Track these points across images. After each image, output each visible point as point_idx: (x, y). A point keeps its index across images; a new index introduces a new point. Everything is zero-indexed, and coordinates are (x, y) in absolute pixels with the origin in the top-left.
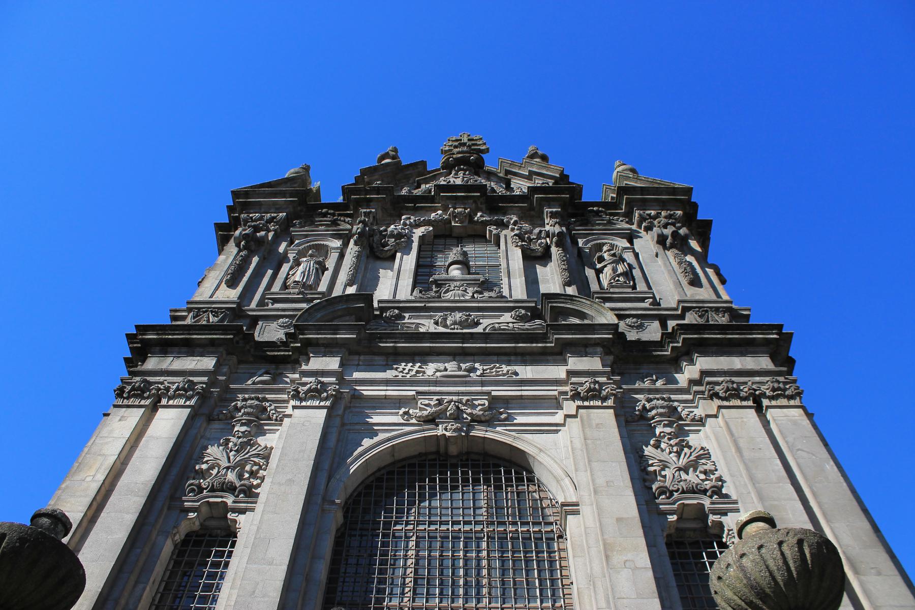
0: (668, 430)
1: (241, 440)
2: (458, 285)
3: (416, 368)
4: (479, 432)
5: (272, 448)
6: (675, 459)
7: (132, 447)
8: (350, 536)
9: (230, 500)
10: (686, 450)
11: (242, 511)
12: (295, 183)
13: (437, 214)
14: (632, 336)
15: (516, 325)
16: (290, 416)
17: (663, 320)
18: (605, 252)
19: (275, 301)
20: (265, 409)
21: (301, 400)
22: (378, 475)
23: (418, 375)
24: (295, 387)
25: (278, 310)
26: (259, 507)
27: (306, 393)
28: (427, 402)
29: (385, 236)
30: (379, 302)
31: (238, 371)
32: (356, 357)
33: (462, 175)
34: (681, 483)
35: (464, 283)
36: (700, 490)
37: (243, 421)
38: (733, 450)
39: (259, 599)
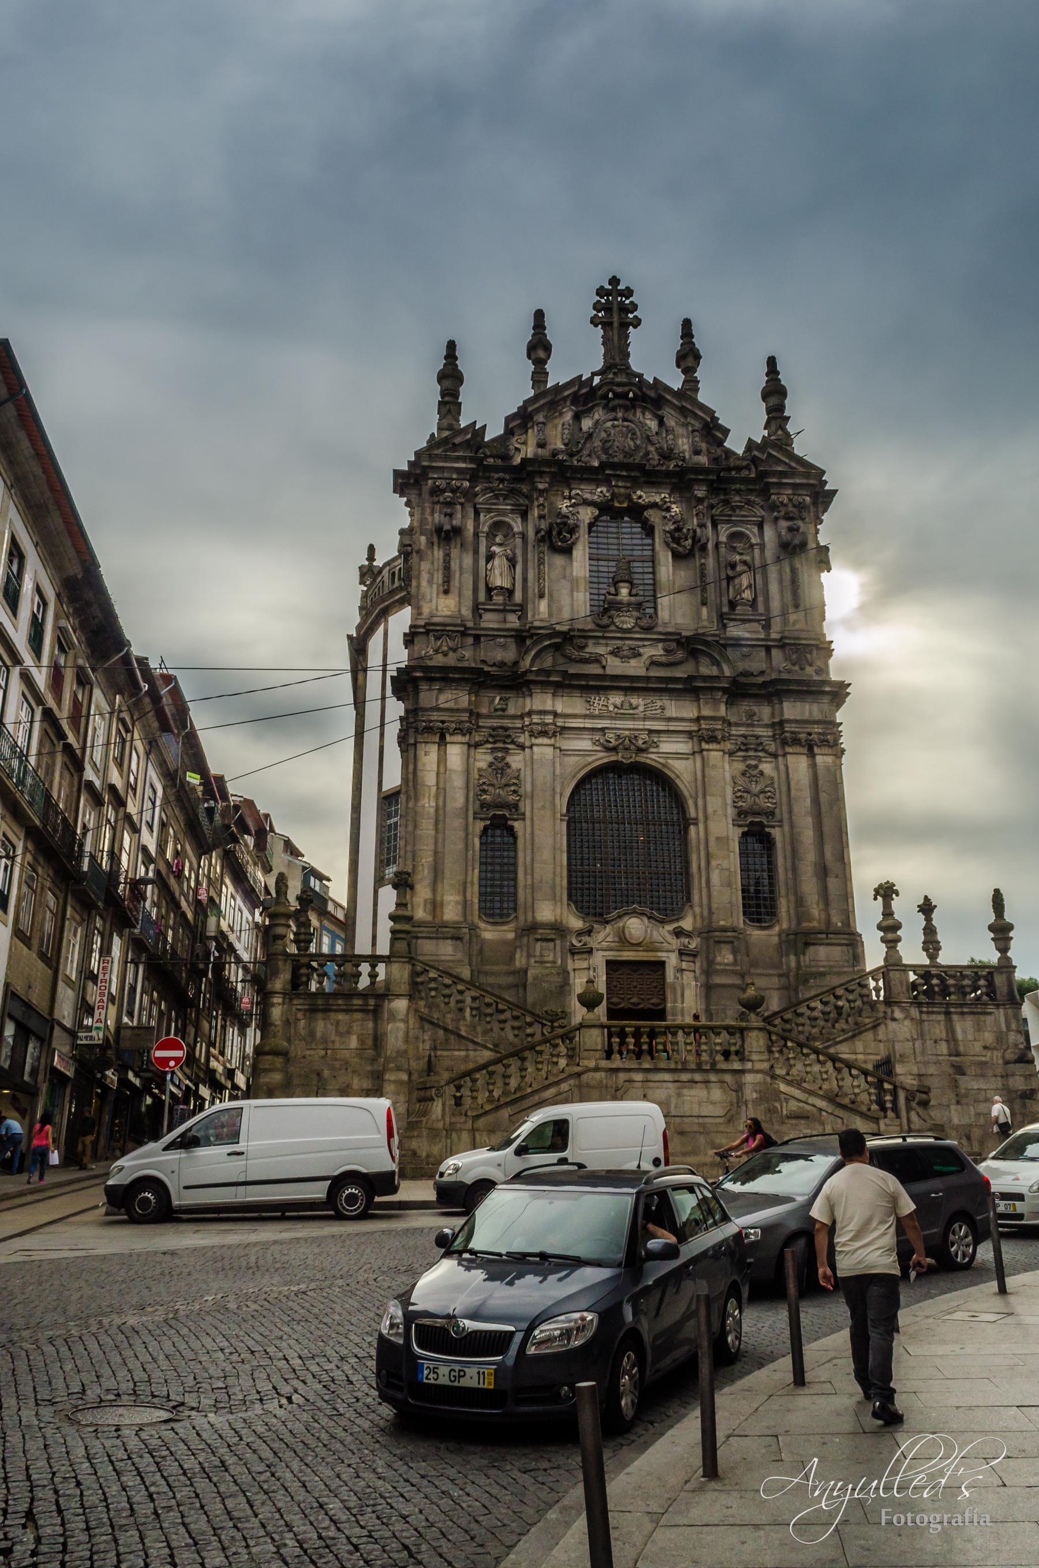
3: (601, 703)
4: (642, 758)
12: (466, 434)
17: (768, 649)
20: (509, 736)
26: (528, 822)
28: (611, 735)
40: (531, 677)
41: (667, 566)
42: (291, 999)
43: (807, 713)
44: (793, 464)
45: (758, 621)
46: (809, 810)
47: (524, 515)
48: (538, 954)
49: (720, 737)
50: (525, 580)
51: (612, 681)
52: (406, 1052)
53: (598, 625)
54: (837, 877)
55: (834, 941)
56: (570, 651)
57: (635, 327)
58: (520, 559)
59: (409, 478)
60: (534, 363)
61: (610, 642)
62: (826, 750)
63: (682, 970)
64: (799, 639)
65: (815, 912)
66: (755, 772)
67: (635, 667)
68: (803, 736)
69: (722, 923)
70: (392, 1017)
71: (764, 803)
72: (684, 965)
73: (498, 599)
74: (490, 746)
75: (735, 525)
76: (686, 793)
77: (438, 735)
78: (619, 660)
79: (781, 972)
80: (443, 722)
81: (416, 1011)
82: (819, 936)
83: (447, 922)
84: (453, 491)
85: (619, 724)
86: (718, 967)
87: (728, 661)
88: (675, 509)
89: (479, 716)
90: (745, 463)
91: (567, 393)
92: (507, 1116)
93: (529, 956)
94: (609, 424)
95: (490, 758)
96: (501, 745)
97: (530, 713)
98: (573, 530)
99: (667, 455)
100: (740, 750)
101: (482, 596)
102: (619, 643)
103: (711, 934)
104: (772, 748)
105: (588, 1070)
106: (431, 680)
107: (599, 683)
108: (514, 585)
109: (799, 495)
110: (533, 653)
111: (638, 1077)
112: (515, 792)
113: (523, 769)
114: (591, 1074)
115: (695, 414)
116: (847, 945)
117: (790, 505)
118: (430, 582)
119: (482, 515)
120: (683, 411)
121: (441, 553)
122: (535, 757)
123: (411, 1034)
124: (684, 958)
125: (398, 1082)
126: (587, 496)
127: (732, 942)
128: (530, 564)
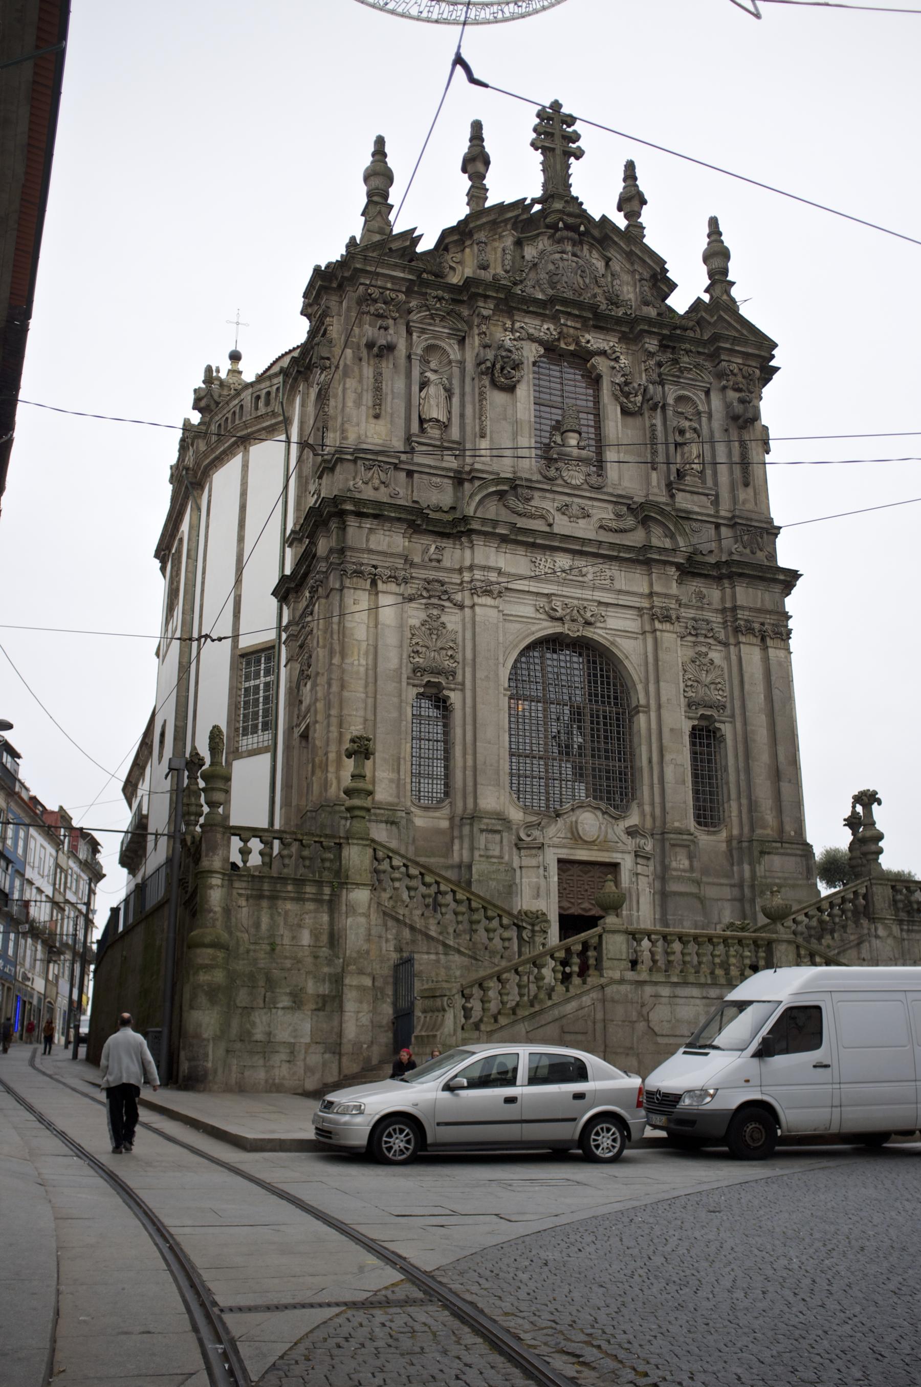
4: (589, 633)
9: (442, 680)
17: (718, 526)
20: (446, 592)
28: (558, 603)
32: (504, 545)
40: (475, 526)
41: (617, 422)
42: (231, 881)
43: (759, 601)
44: (745, 332)
45: (707, 495)
46: (763, 706)
47: (462, 341)
48: (482, 847)
49: (674, 617)
50: (462, 416)
51: (560, 542)
52: (368, 952)
53: (545, 477)
54: (790, 782)
55: (789, 851)
56: (512, 501)
57: (577, 158)
58: (457, 391)
59: (331, 281)
60: (470, 178)
61: (557, 497)
62: (780, 644)
63: (637, 874)
64: (751, 520)
65: (770, 818)
66: (704, 661)
67: (584, 529)
68: (756, 626)
69: (677, 824)
70: (352, 909)
71: (716, 696)
72: (640, 869)
73: (434, 432)
74: (424, 601)
75: (683, 388)
76: (635, 677)
77: (369, 581)
78: (565, 518)
79: (732, 882)
80: (375, 567)
81: (379, 904)
82: (774, 844)
83: (381, 803)
84: (385, 303)
85: (566, 591)
86: (674, 873)
87: (684, 534)
88: (623, 360)
89: (412, 565)
90: (691, 324)
91: (510, 215)
92: (523, 1031)
93: (472, 849)
94: (558, 256)
95: (423, 615)
96: (435, 601)
97: (471, 568)
98: (517, 366)
99: (614, 300)
100: (690, 634)
101: (415, 427)
102: (566, 498)
103: (666, 836)
104: (722, 636)
105: (612, 982)
106: (360, 515)
107: (547, 543)
108: (449, 419)
109: (749, 366)
110: (477, 498)
111: (665, 991)
113: (460, 631)
114: (615, 987)
115: (644, 262)
116: (801, 856)
117: (740, 375)
118: (358, 403)
119: (414, 334)
120: (630, 255)
121: (371, 370)
122: (477, 619)
123: (373, 932)
124: (639, 860)
125: (361, 988)
126: (531, 331)
127: (688, 846)
128: (468, 398)
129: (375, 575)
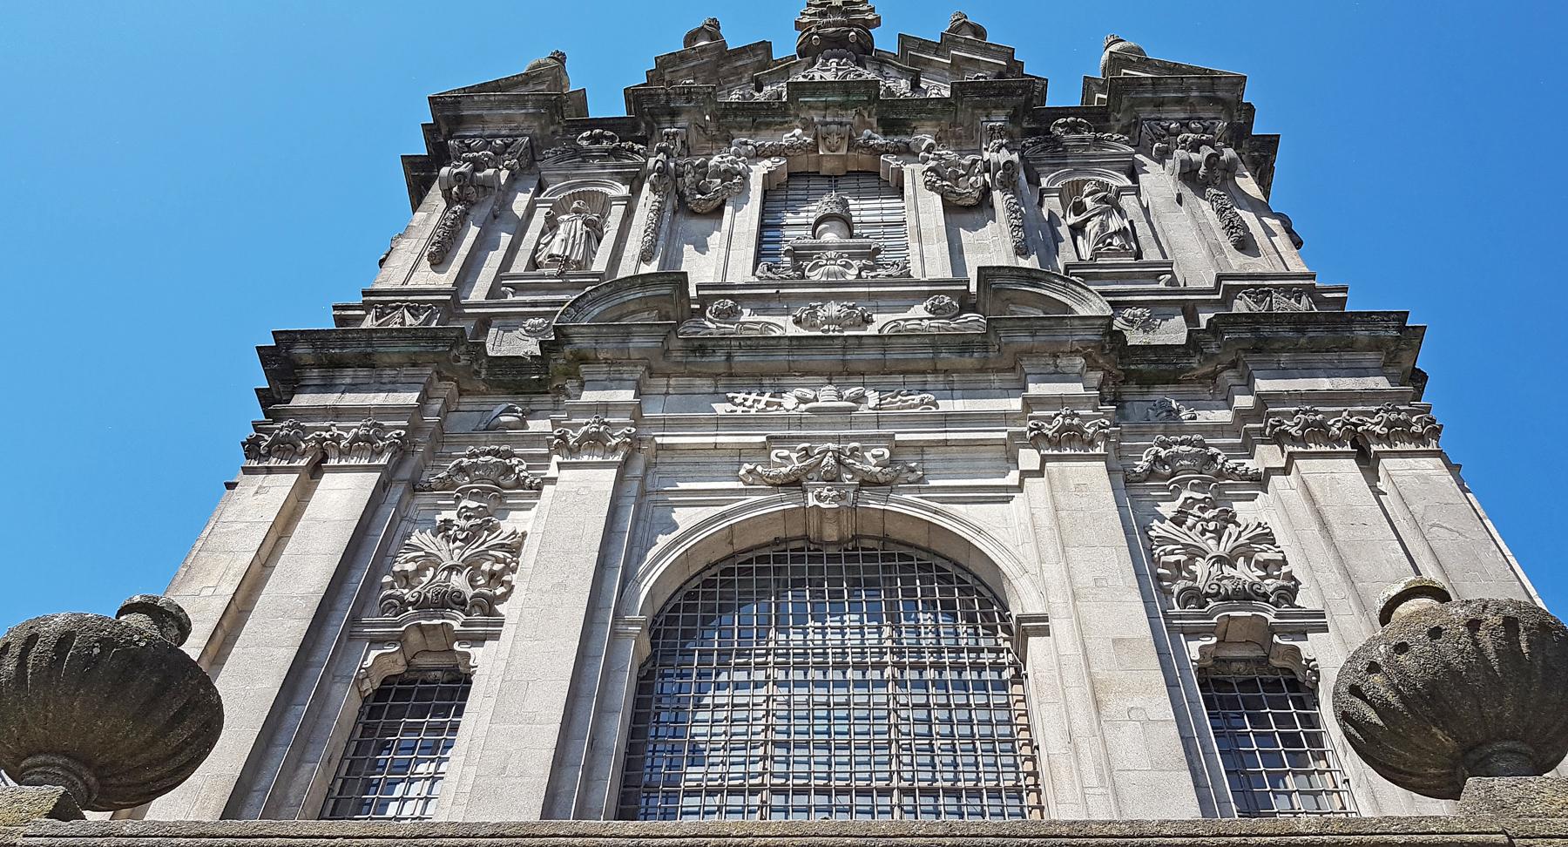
0: (1200, 496)
1: (472, 522)
2: (833, 257)
3: (767, 397)
5: (524, 535)
6: (1212, 543)
7: (279, 538)
8: (663, 676)
10: (1232, 527)
11: (479, 640)
12: (543, 83)
13: (794, 136)
14: (1135, 338)
15: (934, 323)
16: (553, 481)
17: (1190, 314)
18: (1087, 196)
19: (518, 289)
20: (511, 469)
21: (572, 451)
22: (706, 575)
23: (768, 409)
24: (560, 432)
25: (525, 304)
26: (507, 632)
27: (580, 441)
28: (786, 453)
29: (705, 175)
30: (699, 287)
31: (461, 408)
32: (664, 381)
33: (834, 65)
34: (1225, 582)
35: (843, 253)
36: (1257, 594)
37: (475, 490)
38: (1316, 527)
39: (513, 780)
40: (581, 343)
112: (494, 577)
129: (325, 439)
